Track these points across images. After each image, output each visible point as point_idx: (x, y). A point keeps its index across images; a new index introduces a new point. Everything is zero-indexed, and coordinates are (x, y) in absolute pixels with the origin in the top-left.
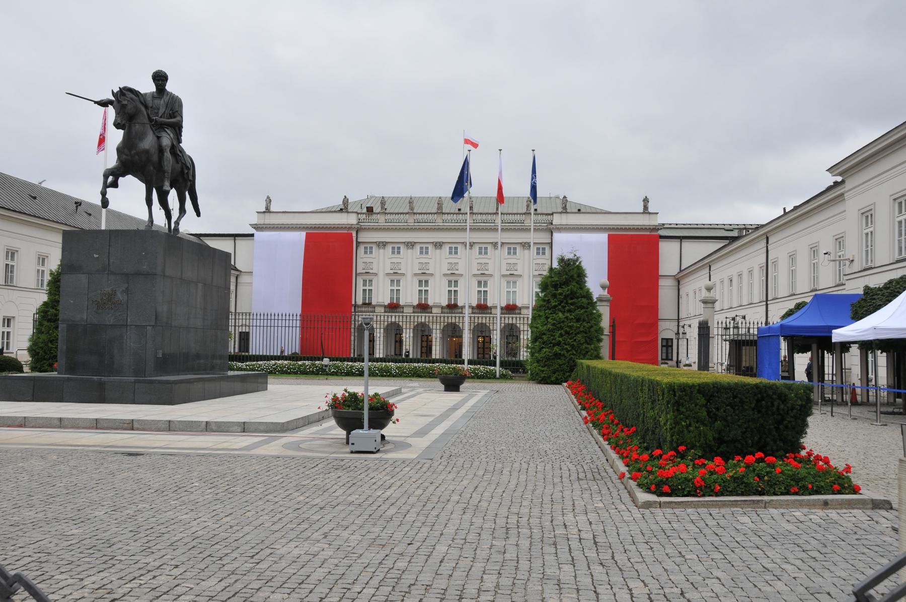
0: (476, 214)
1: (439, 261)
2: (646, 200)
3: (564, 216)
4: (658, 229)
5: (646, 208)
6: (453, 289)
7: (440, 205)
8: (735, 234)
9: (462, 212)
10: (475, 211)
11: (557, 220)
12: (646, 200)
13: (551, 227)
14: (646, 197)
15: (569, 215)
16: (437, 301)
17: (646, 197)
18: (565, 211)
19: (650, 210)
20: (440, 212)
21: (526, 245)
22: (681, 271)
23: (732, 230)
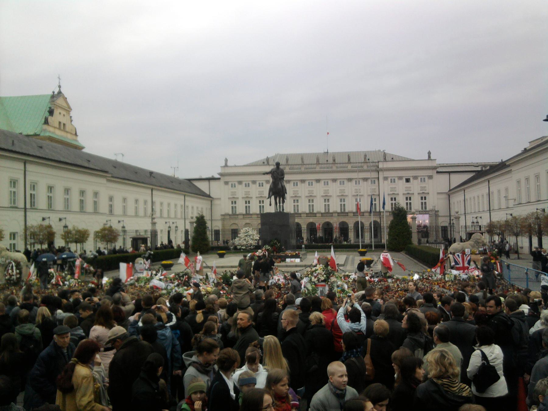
0: (337, 164)
1: (319, 190)
2: (429, 153)
3: (385, 163)
4: (436, 168)
5: (429, 157)
6: (327, 203)
7: (318, 160)
8: (479, 169)
9: (328, 162)
10: (336, 162)
11: (381, 166)
12: (429, 153)
13: (378, 169)
14: (429, 151)
15: (387, 162)
16: (319, 210)
17: (429, 151)
18: (385, 160)
19: (432, 158)
20: (318, 163)
21: (365, 179)
22: (450, 190)
23: (478, 166)
